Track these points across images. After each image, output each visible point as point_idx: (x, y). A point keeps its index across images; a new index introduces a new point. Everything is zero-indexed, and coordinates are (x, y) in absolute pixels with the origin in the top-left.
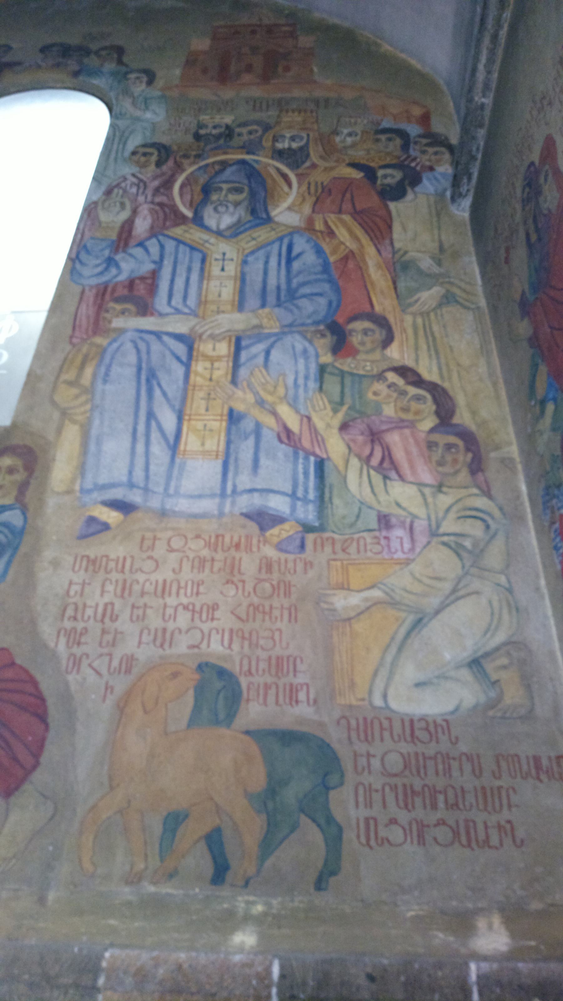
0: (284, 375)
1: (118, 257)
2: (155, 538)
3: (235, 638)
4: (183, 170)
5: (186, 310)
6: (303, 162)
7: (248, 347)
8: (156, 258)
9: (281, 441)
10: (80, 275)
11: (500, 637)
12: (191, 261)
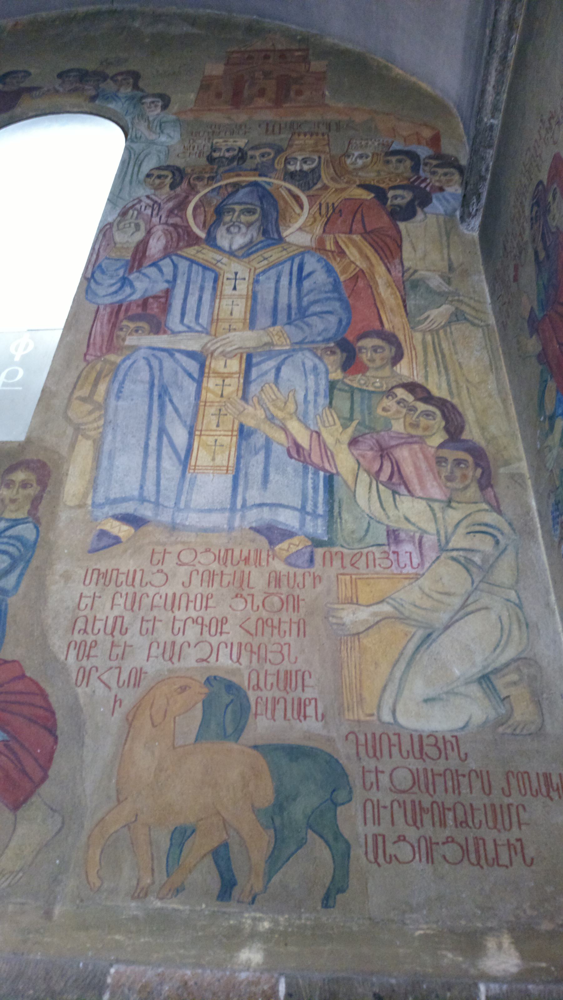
0: (295, 391)
1: (132, 277)
3: (243, 651)
4: (198, 192)
5: (198, 328)
6: (315, 184)
7: (258, 364)
8: (170, 278)
9: (291, 457)
10: (96, 294)
11: (510, 653)
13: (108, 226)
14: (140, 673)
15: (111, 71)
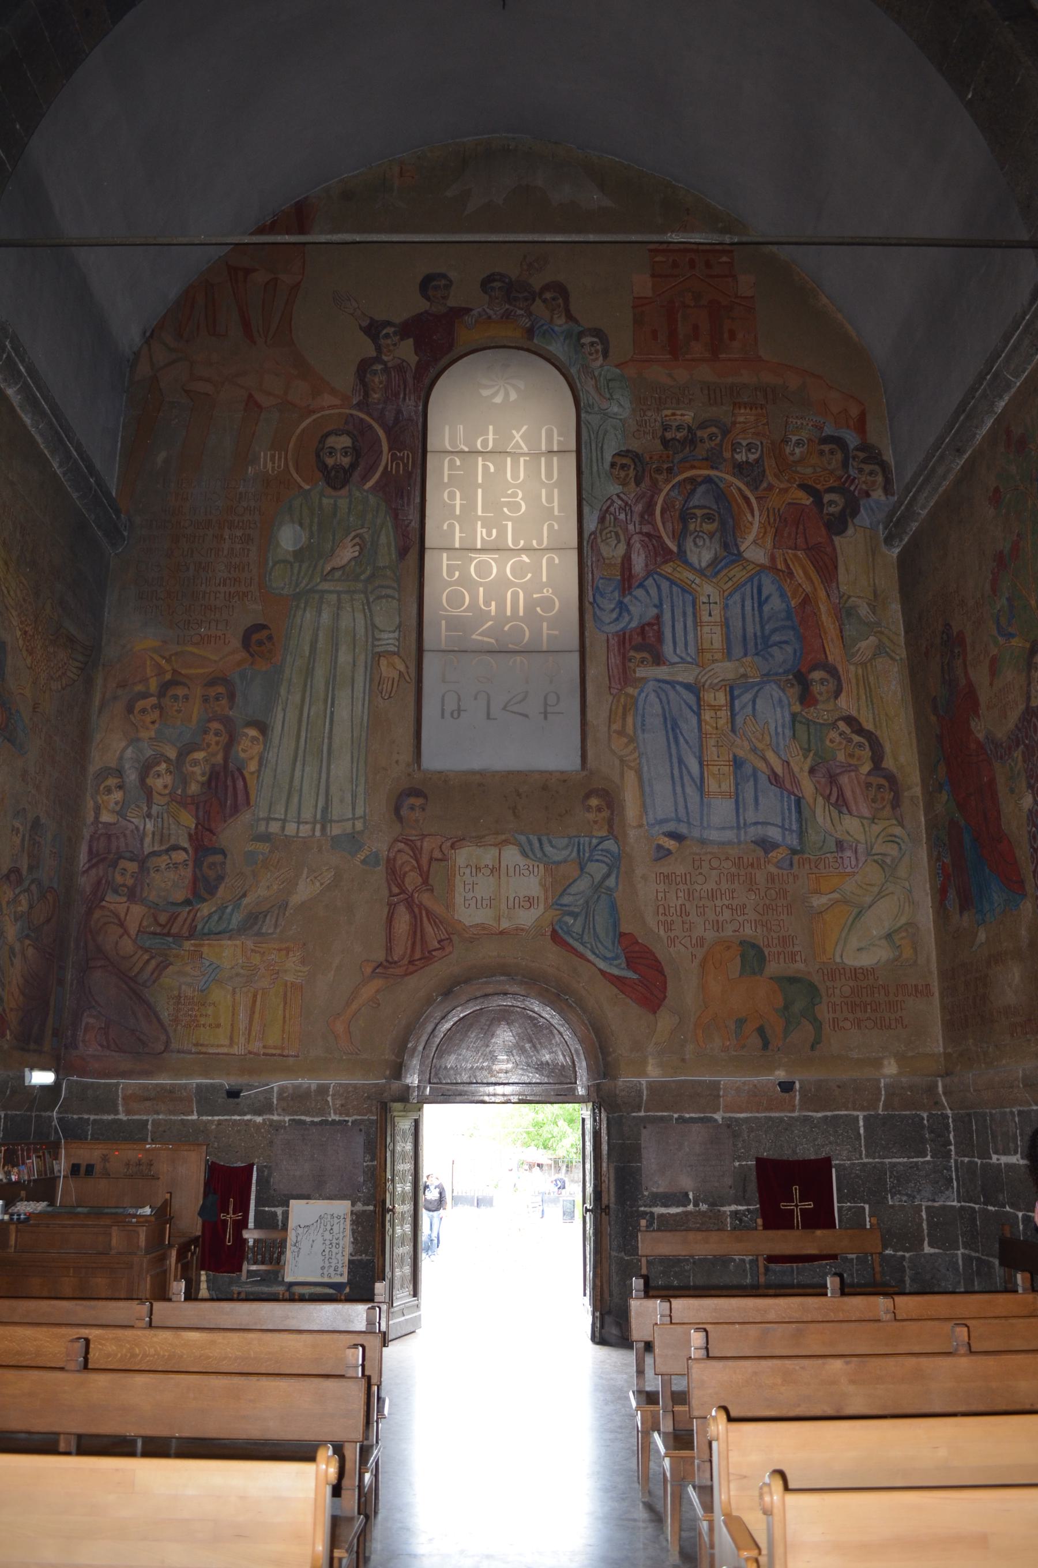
0: (767, 723)
1: (626, 600)
4: (661, 490)
5: (689, 659)
6: (761, 481)
7: (739, 696)
8: (656, 601)
9: (772, 784)
11: (903, 920)
12: (684, 602)
13: (593, 537)
14: (702, 940)
15: (537, 282)
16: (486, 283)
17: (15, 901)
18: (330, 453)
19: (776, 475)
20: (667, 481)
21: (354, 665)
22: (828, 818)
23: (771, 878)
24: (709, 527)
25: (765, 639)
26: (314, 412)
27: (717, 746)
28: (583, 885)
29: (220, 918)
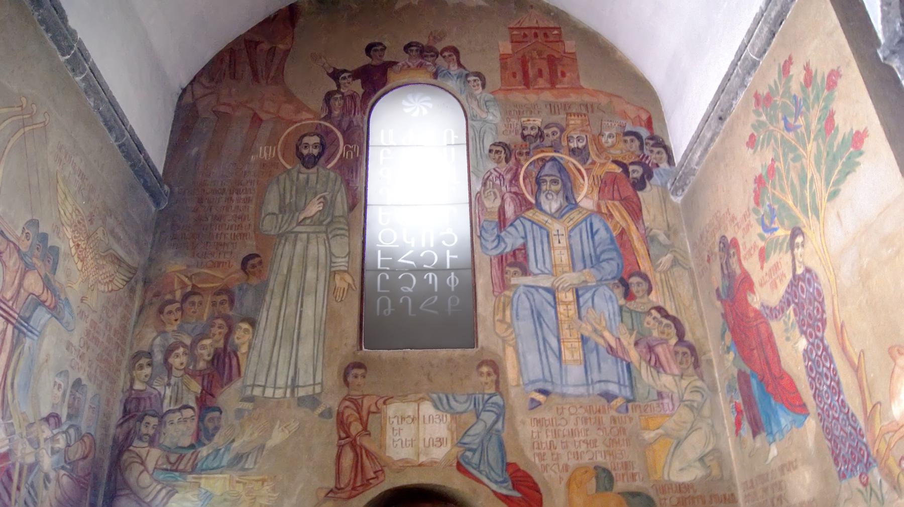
1: (503, 234)
2: (563, 408)
4: (522, 166)
5: (546, 271)
6: (588, 159)
7: (583, 294)
8: (522, 234)
10: (487, 249)
11: (710, 448)
14: (566, 467)
15: (439, 47)
16: (407, 48)
17: (53, 439)
18: (306, 147)
19: (596, 155)
20: (526, 160)
21: (317, 280)
22: (650, 376)
23: (614, 420)
24: (554, 187)
25: (598, 258)
26: (296, 122)
27: (569, 328)
28: (479, 428)
29: (215, 458)
